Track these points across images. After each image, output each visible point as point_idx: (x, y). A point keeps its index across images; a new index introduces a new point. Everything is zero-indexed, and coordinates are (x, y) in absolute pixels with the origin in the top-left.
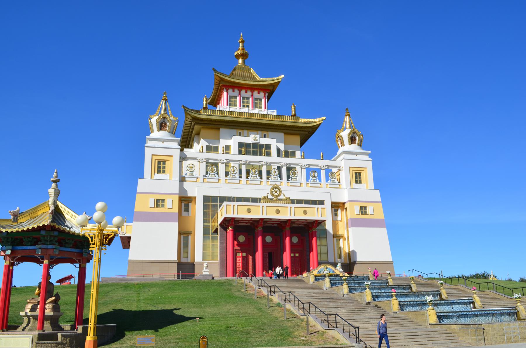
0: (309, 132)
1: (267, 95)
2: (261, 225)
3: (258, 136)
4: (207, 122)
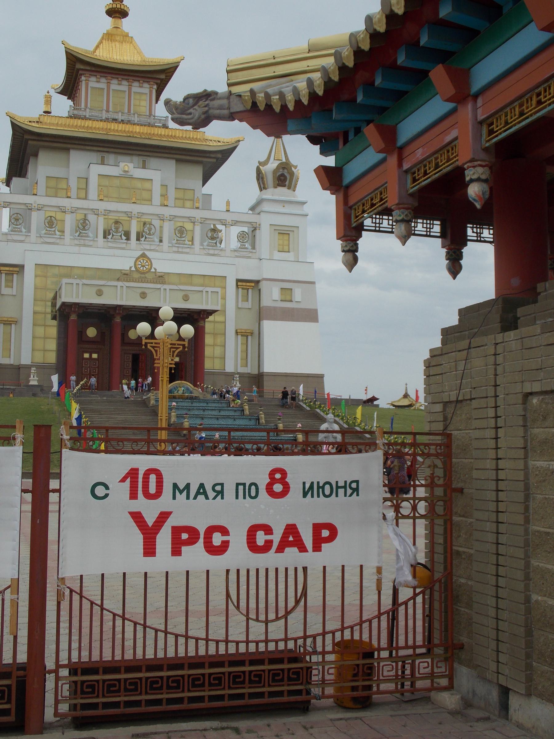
0: (217, 159)
1: (155, 87)
2: (119, 314)
3: (131, 165)
4: (47, 139)
